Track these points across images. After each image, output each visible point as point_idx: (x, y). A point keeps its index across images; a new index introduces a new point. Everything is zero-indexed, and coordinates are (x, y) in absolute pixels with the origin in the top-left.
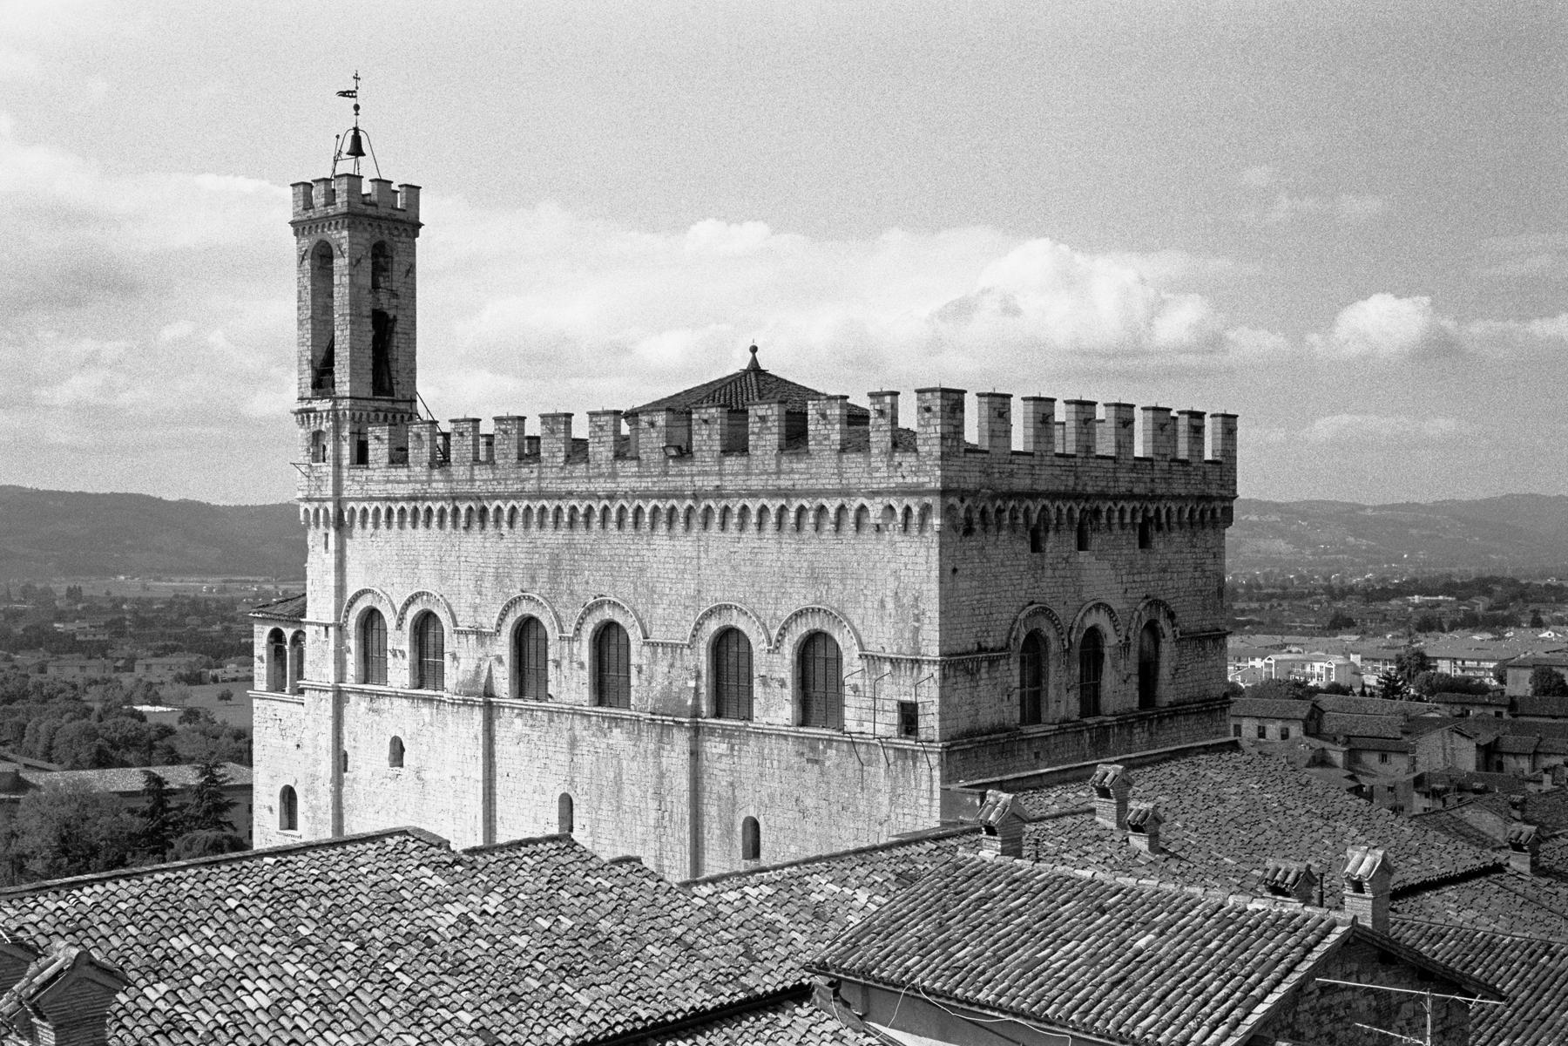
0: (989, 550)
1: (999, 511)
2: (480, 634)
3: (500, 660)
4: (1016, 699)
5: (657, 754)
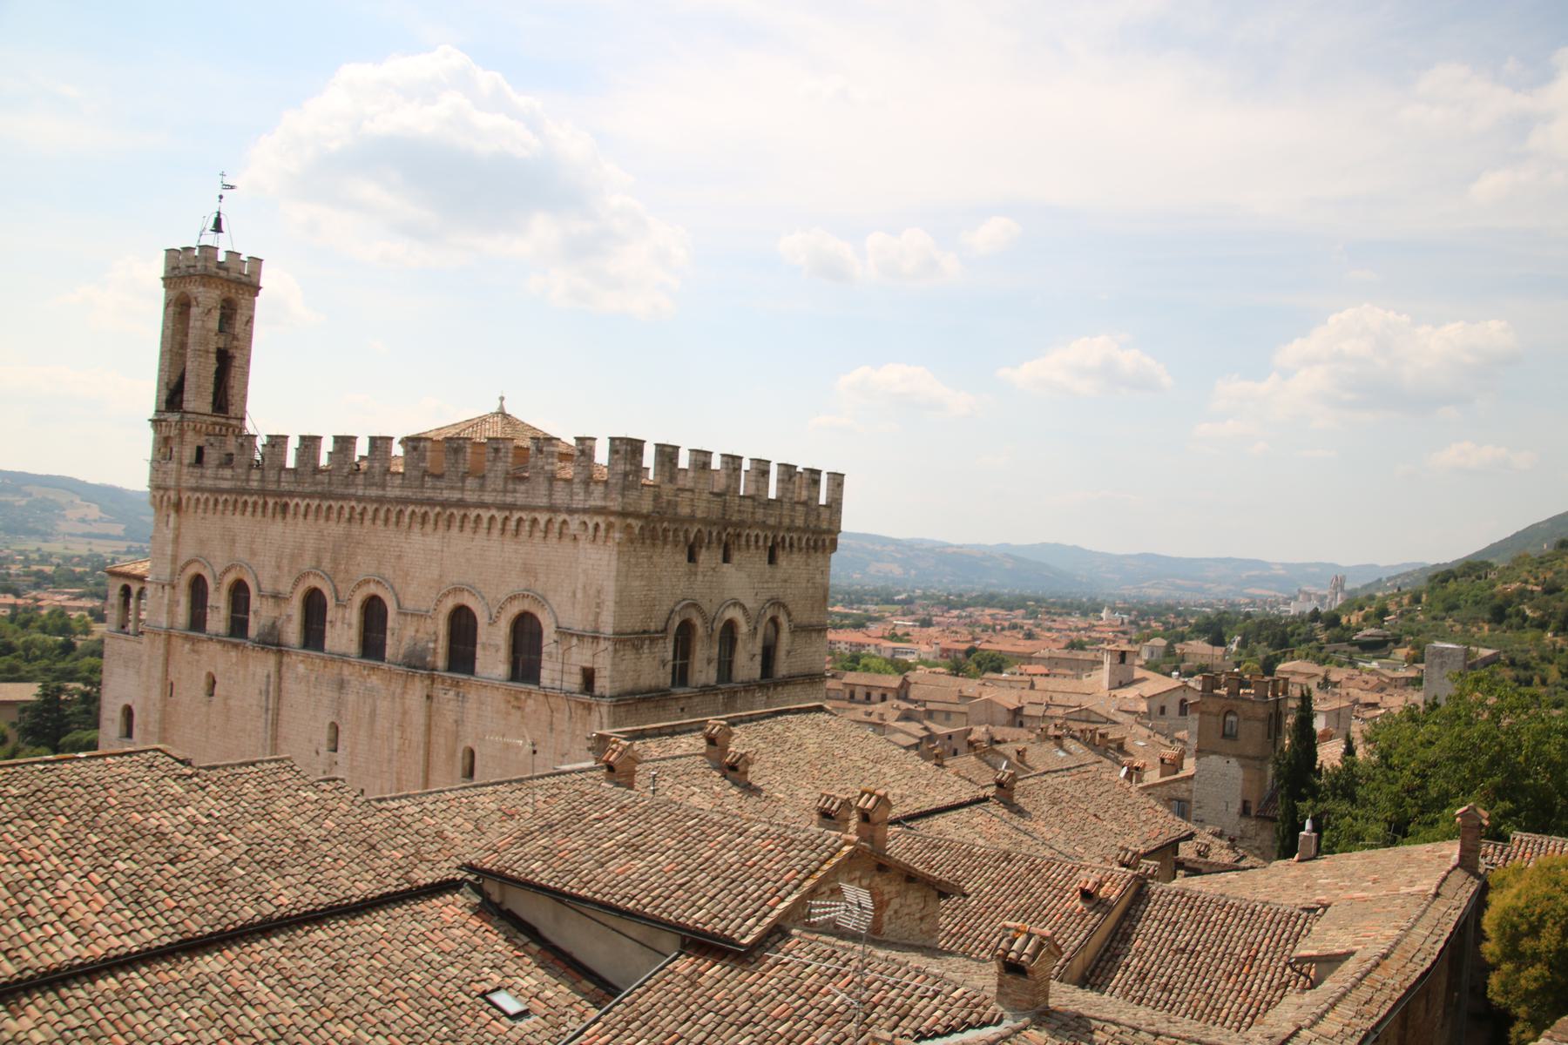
0: (656, 559)
1: (665, 530)
2: (276, 596)
3: (289, 617)
4: (669, 668)
5: (404, 693)
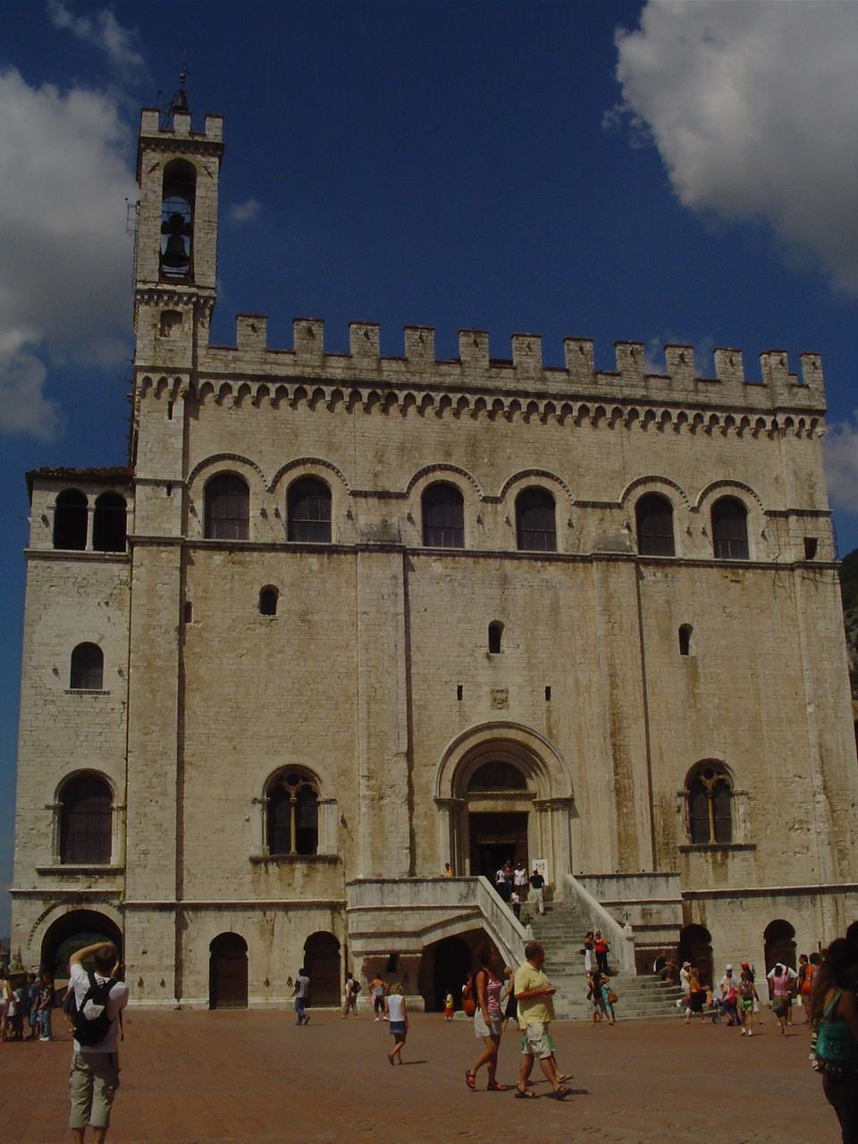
2: (384, 495)
3: (410, 518)
